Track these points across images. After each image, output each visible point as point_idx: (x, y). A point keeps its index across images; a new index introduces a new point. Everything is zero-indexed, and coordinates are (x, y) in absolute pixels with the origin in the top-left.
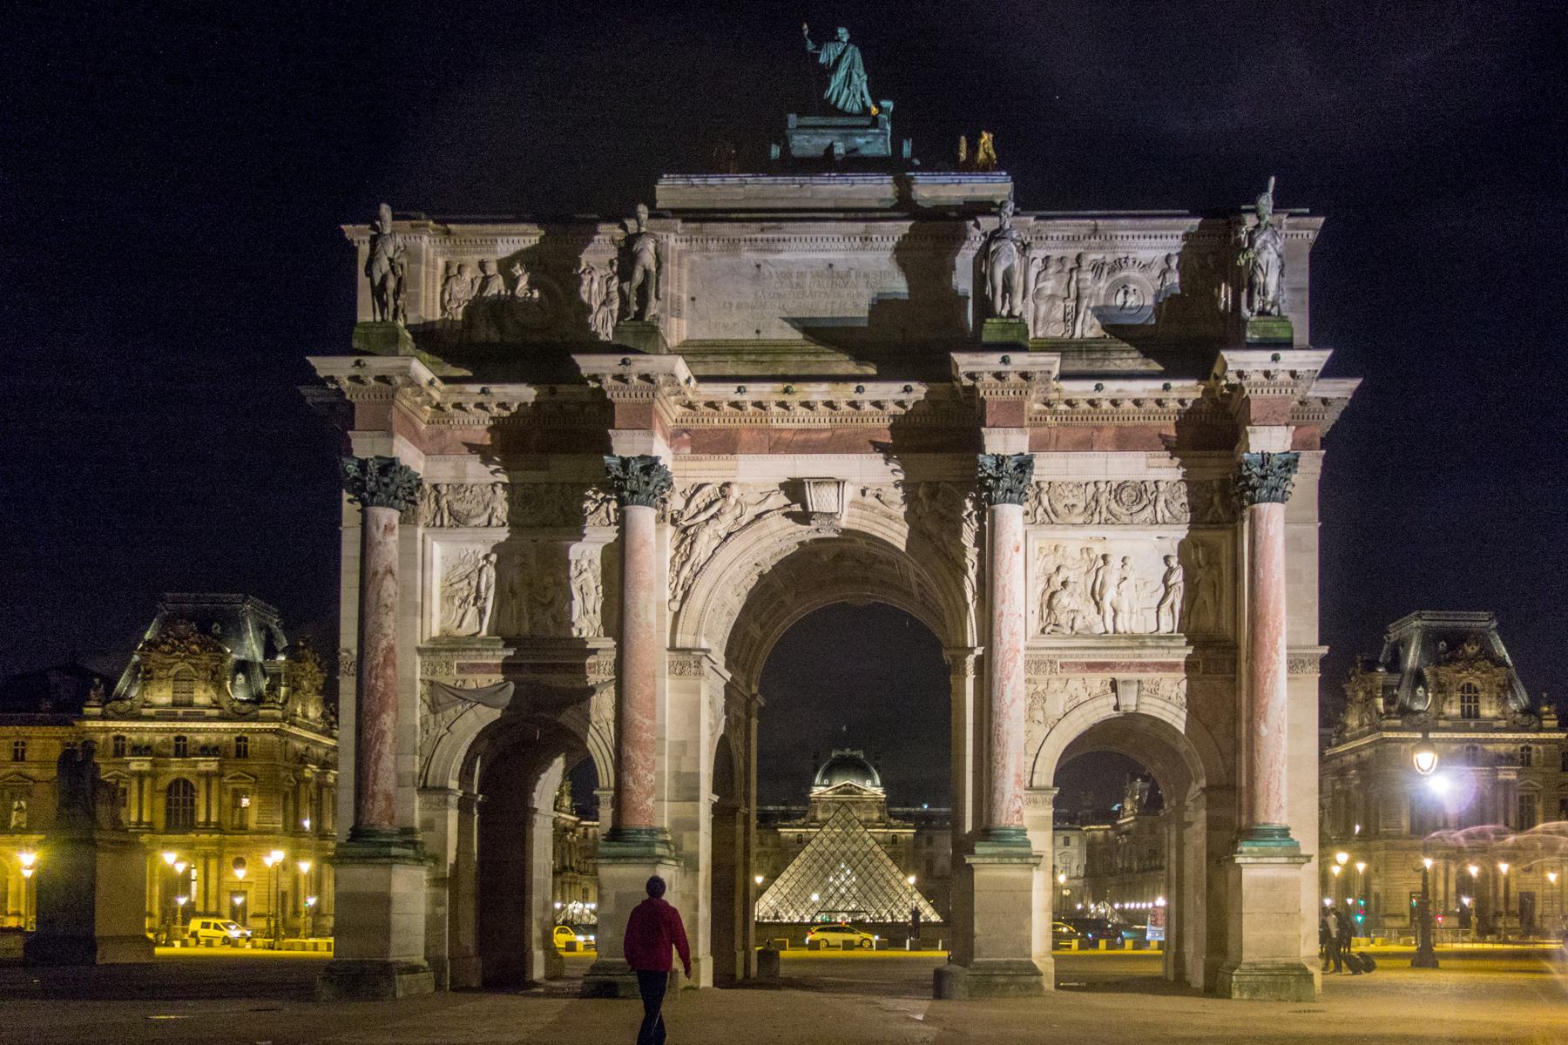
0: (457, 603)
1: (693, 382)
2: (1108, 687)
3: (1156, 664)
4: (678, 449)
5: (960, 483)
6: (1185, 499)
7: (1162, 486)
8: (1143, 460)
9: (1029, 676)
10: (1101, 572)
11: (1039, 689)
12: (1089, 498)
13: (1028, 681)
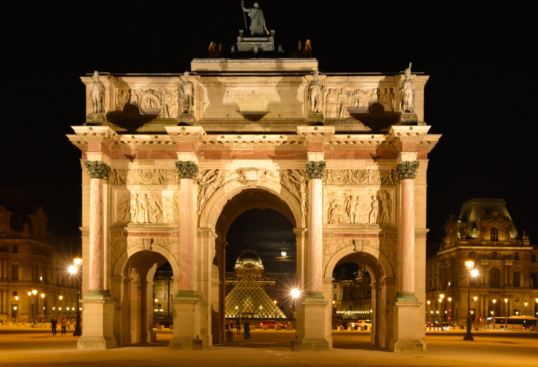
0: (123, 211)
1: (206, 134)
2: (352, 242)
3: (369, 234)
4: (200, 157)
6: (379, 177)
7: (371, 171)
8: (365, 162)
9: (324, 238)
10: (349, 202)
11: (327, 243)
12: (345, 175)
13: (323, 240)
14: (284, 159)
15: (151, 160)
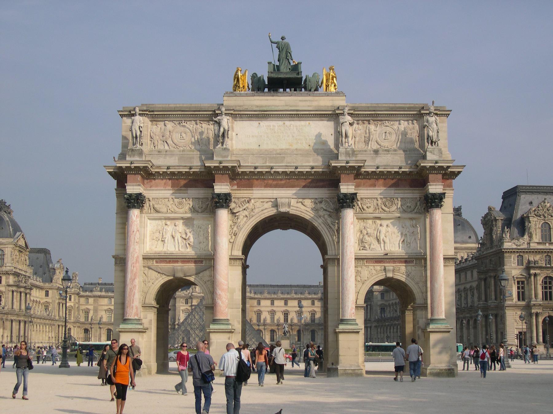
5: (331, 198)
14: (315, 188)
15: (184, 189)
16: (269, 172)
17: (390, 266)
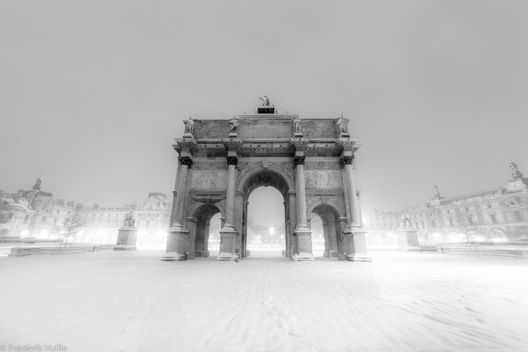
3: (328, 195)
8: (323, 158)
16: (258, 148)
17: (324, 198)
